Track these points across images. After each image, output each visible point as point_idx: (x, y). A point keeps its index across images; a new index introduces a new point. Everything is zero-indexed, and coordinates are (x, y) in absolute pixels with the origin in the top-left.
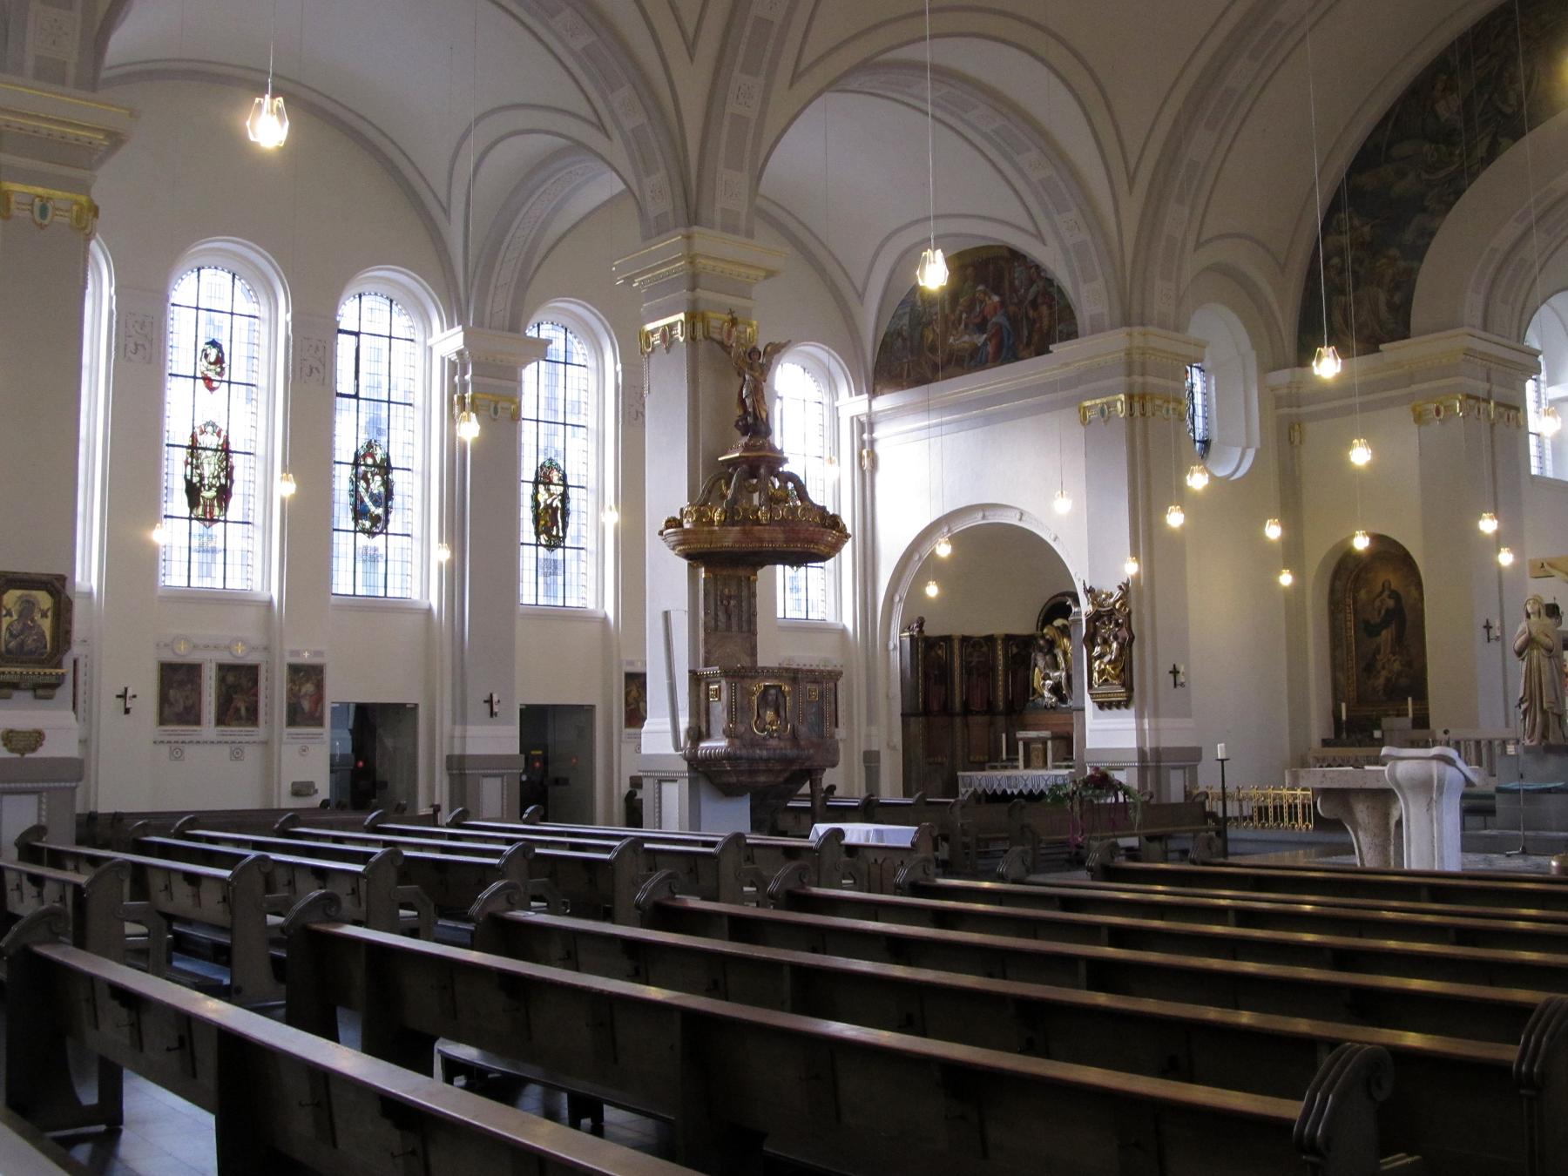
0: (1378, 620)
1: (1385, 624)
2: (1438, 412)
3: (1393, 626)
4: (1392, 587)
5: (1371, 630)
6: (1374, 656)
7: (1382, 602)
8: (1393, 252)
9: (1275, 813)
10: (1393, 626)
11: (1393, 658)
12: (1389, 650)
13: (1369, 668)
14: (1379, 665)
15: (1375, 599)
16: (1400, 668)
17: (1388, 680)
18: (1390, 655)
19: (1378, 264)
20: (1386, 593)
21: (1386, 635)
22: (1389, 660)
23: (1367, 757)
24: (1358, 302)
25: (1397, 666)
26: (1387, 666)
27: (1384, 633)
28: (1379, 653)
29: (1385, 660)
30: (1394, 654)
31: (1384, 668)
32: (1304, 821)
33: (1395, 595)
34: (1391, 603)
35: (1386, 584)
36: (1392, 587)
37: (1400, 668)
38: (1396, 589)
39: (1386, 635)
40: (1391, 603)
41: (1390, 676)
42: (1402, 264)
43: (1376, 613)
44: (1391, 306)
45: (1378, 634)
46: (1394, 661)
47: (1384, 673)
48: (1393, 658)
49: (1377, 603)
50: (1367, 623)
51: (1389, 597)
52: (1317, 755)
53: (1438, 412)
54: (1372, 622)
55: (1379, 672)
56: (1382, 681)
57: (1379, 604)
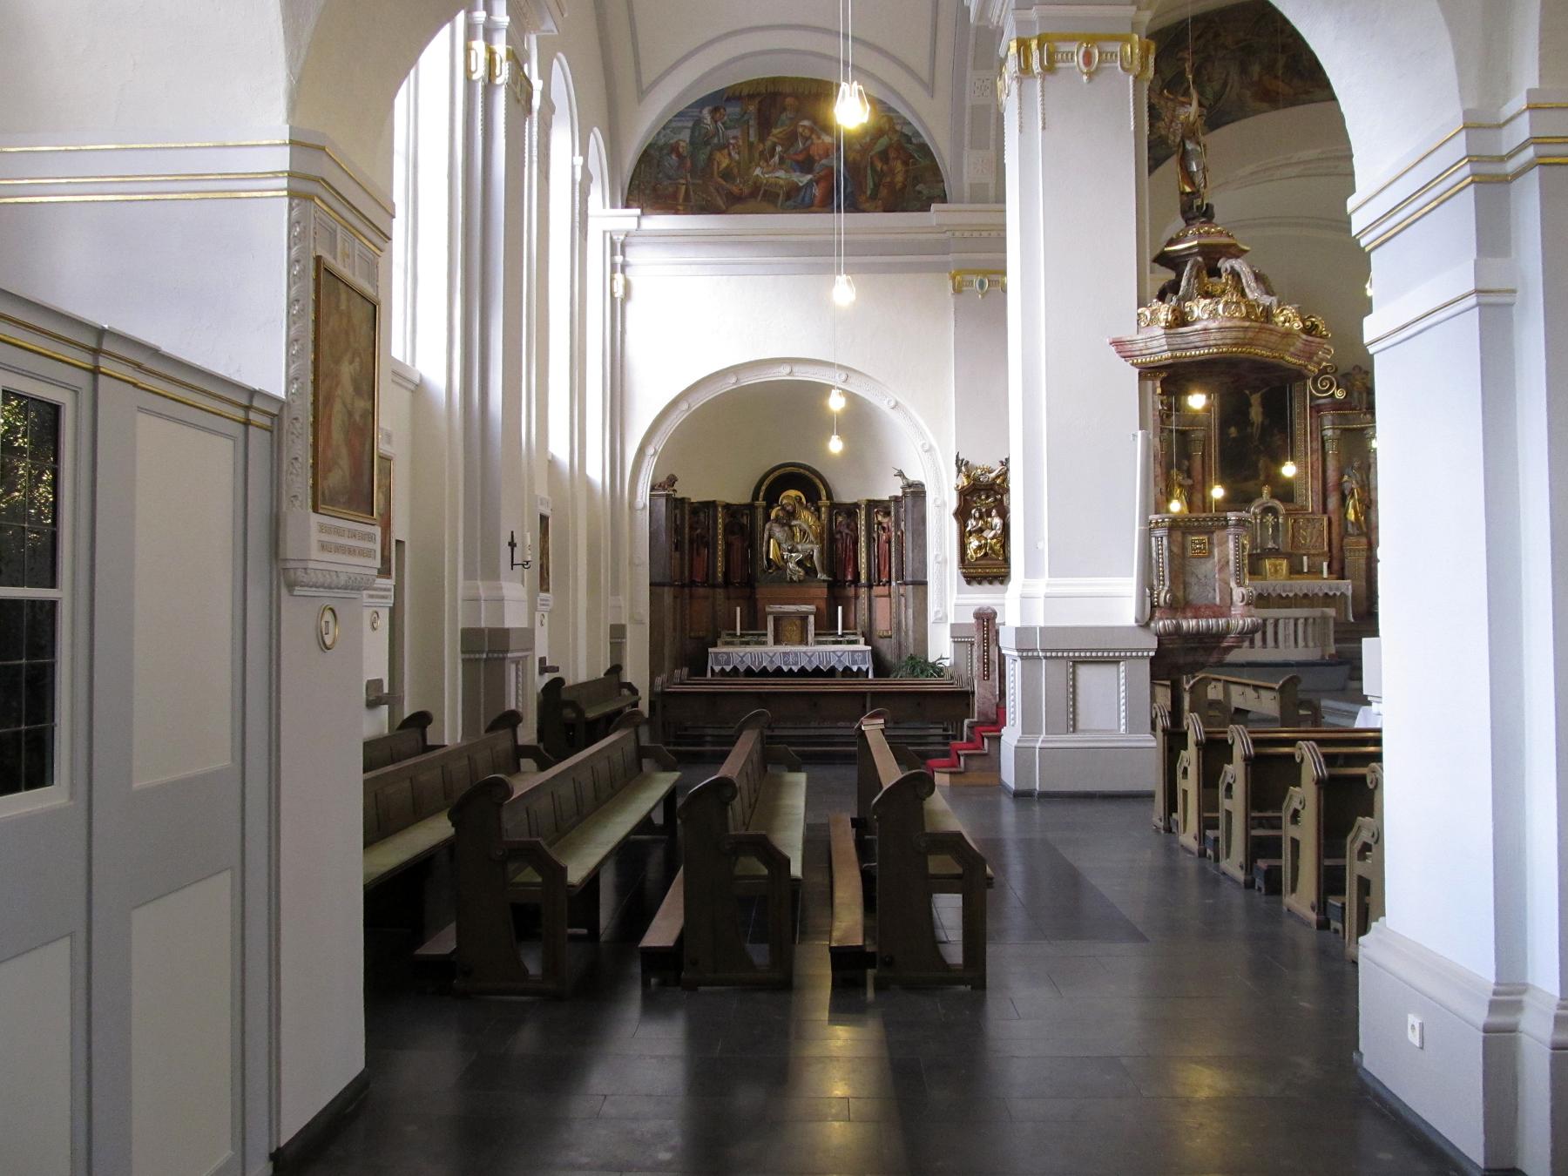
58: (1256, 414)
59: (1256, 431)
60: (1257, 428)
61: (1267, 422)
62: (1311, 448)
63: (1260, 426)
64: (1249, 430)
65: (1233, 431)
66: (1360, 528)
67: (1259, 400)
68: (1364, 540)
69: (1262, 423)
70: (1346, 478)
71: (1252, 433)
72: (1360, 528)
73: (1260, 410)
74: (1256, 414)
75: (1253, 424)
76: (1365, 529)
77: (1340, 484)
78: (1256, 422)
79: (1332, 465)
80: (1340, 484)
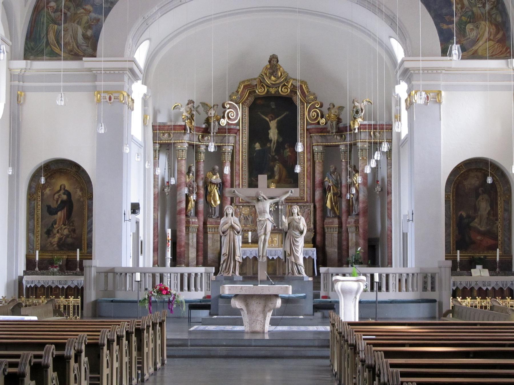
0: (56, 206)
1: (60, 208)
2: (110, 99)
3: (65, 209)
4: (66, 189)
5: (51, 211)
6: (52, 226)
7: (59, 196)
8: (89, 7)
9: (74, 309)
10: (65, 209)
11: (65, 227)
12: (61, 223)
13: (49, 232)
14: (55, 231)
15: (54, 195)
16: (68, 233)
17: (60, 239)
18: (62, 226)
19: (78, 12)
20: (62, 191)
21: (61, 215)
22: (62, 228)
23: (60, 281)
24: (66, 30)
25: (66, 232)
26: (60, 231)
27: (59, 213)
28: (55, 224)
29: (59, 228)
30: (65, 225)
31: (58, 232)
32: (74, 314)
33: (68, 194)
34: (65, 197)
35: (62, 187)
36: (66, 189)
37: (68, 233)
38: (67, 190)
39: (61, 215)
40: (65, 197)
41: (61, 237)
42: (93, 15)
43: (55, 202)
44: (85, 37)
45: (57, 214)
46: (65, 228)
47: (58, 235)
48: (65, 227)
49: (56, 196)
50: (49, 207)
51: (64, 194)
52: (28, 280)
53: (110, 99)
54: (52, 206)
55: (55, 234)
56: (56, 239)
57: (58, 197)
58: (273, 134)
59: (273, 146)
60: (274, 144)
61: (281, 140)
62: (307, 157)
63: (275, 142)
64: (268, 145)
65: (257, 146)
66: (334, 213)
67: (275, 125)
68: (336, 220)
69: (278, 141)
70: (326, 179)
71: (270, 147)
72: (334, 213)
73: (276, 131)
74: (273, 134)
75: (271, 141)
76: (338, 214)
77: (322, 183)
78: (273, 139)
79: (318, 169)
80: (322, 183)
